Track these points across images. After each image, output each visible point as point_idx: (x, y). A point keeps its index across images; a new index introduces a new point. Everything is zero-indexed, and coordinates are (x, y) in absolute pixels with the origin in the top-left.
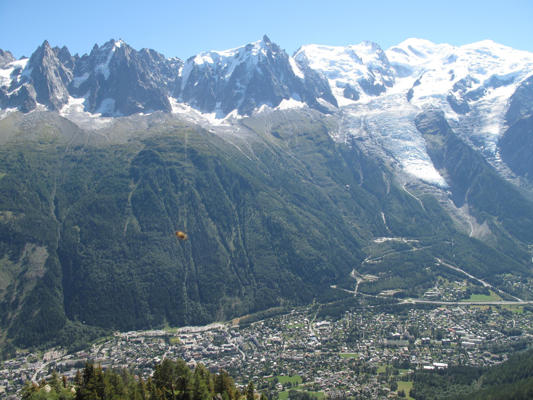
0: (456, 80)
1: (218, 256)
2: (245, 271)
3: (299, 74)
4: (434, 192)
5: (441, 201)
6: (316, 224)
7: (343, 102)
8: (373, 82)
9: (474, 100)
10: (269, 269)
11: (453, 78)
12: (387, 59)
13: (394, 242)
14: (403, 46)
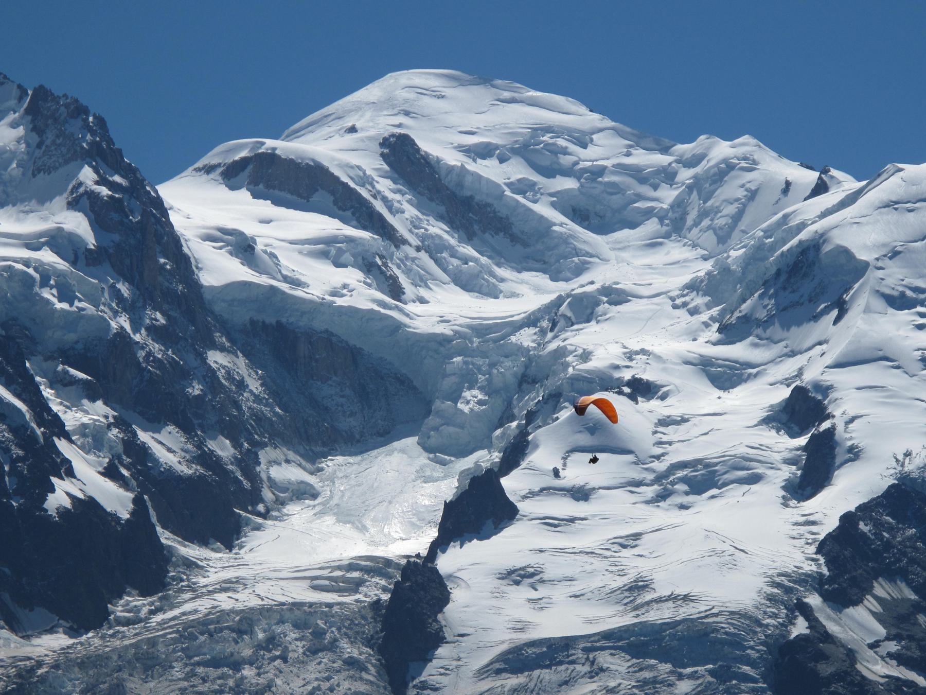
12: (184, 265)
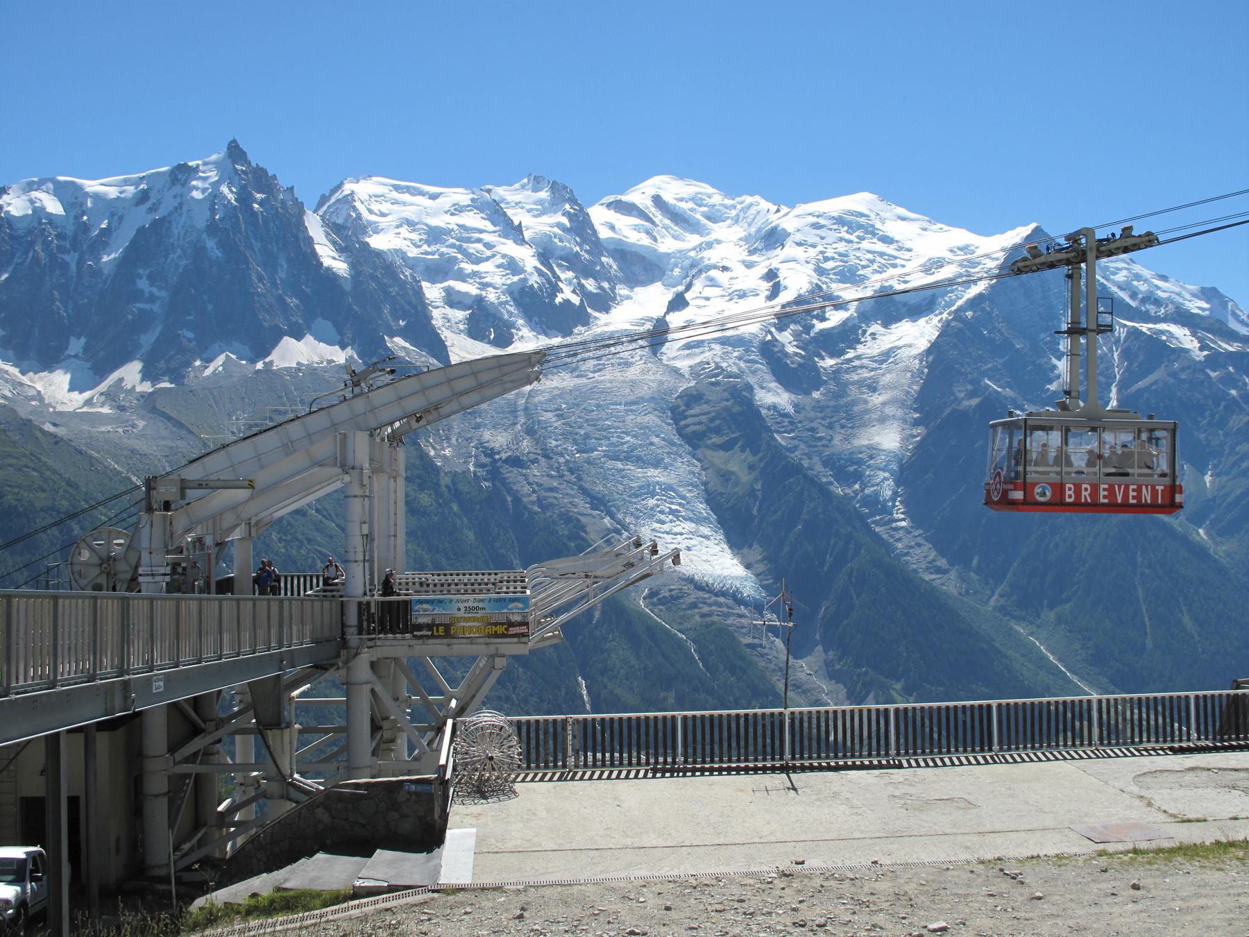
0: (785, 297)
4: (727, 615)
5: (748, 640)
9: (832, 356)
11: (775, 292)
12: (595, 232)
14: (640, 195)
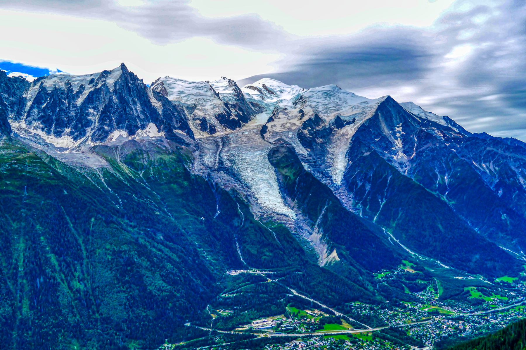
0: (306, 118)
1: (58, 297)
2: (89, 312)
3: (157, 104)
5: (294, 232)
6: (170, 257)
7: (198, 134)
8: (229, 117)
10: (116, 309)
13: (249, 274)
